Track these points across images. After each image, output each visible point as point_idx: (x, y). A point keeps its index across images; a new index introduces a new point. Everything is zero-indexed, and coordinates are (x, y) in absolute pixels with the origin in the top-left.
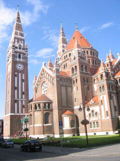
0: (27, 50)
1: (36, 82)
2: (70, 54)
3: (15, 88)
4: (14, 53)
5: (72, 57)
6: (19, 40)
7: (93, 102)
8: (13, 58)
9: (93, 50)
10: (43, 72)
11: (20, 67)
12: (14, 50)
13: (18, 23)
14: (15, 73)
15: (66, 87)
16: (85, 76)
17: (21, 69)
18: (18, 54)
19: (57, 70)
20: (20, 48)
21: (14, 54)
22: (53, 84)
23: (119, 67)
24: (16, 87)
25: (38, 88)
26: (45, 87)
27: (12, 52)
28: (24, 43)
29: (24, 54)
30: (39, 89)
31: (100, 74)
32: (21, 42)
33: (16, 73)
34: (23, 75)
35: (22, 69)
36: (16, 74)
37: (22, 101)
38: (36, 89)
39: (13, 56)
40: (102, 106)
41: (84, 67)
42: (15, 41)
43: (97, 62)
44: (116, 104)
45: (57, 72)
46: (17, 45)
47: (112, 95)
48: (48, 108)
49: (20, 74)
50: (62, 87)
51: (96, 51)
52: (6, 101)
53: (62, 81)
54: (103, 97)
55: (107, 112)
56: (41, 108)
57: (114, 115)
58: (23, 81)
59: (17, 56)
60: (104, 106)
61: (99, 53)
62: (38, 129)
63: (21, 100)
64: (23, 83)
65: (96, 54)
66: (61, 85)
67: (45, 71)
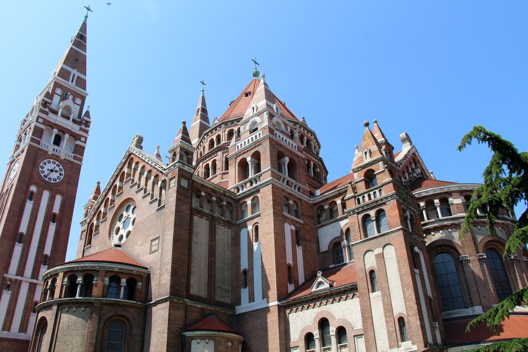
0: (89, 126)
3: (20, 238)
5: (245, 129)
8: (32, 140)
10: (129, 167)
13: (75, 48)
14: (28, 187)
18: (55, 131)
21: (43, 127)
24: (22, 235)
27: (37, 121)
28: (82, 106)
30: (104, 228)
31: (363, 167)
32: (74, 100)
33: (33, 188)
34: (58, 199)
36: (32, 193)
37: (32, 288)
38: (91, 231)
39: (38, 133)
41: (287, 159)
43: (318, 170)
45: (185, 158)
47: (416, 249)
49: (46, 195)
53: (199, 196)
55: (401, 320)
56: (96, 291)
58: (50, 217)
63: (31, 283)
64: (53, 227)
66: (193, 212)
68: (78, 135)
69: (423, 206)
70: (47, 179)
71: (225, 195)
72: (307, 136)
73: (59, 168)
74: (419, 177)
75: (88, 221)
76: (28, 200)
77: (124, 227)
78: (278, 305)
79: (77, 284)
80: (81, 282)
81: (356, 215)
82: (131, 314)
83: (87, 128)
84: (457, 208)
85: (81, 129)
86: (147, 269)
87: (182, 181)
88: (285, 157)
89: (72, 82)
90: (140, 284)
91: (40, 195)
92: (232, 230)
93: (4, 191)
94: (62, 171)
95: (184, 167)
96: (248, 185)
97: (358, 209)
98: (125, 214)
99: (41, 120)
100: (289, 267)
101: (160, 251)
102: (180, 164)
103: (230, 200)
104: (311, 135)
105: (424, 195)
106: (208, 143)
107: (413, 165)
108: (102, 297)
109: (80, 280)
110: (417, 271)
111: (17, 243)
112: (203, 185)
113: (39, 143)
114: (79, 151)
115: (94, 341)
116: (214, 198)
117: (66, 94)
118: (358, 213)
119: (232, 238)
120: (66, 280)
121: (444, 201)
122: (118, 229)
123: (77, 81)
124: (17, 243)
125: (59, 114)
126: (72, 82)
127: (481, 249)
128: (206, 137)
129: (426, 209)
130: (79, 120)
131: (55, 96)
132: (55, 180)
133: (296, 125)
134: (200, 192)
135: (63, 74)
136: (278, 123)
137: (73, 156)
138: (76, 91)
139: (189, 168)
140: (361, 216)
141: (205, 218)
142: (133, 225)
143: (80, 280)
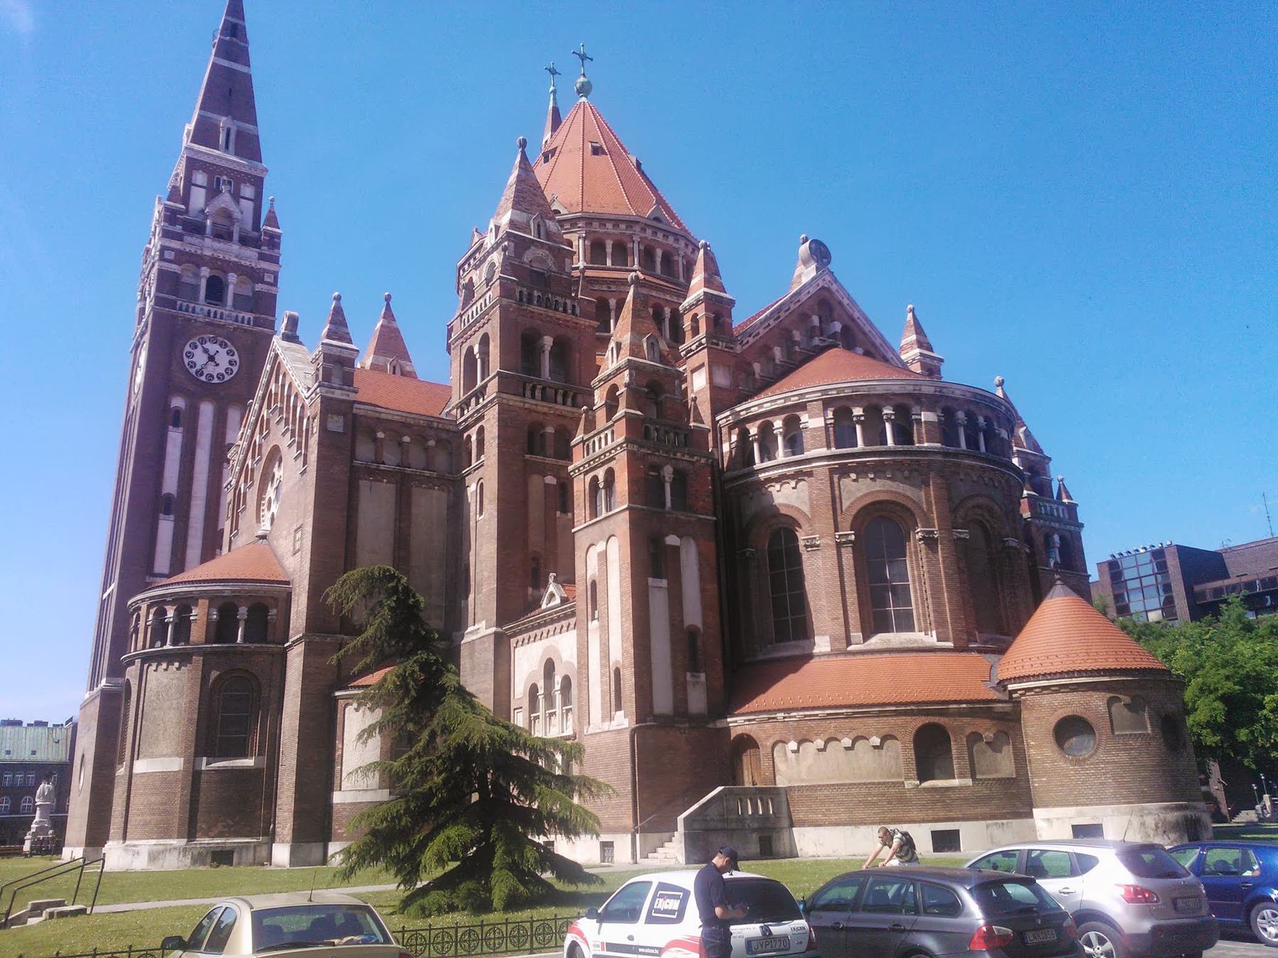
6: (217, 178)
7: (557, 601)
9: (667, 233)
11: (211, 358)
12: (175, 244)
15: (404, 484)
18: (205, 272)
20: (223, 235)
21: (174, 268)
23: (795, 343)
24: (169, 496)
27: (162, 258)
28: (257, 200)
32: (237, 197)
33: (178, 402)
36: (177, 411)
40: (595, 622)
41: (548, 341)
42: (189, 182)
44: (693, 615)
47: (672, 540)
48: (245, 639)
49: (207, 411)
50: (364, 485)
52: (104, 591)
53: (375, 440)
54: (603, 556)
55: (617, 672)
56: (197, 633)
57: (663, 702)
59: (196, 288)
60: (605, 630)
62: (153, 799)
69: (755, 435)
70: (203, 378)
71: (431, 428)
72: (660, 244)
73: (226, 349)
74: (826, 344)
76: (171, 427)
78: (495, 633)
79: (168, 624)
80: (171, 620)
81: (582, 476)
83: (275, 252)
84: (813, 437)
85: (262, 257)
86: (288, 583)
87: (330, 420)
89: (227, 147)
90: (274, 611)
91: (194, 413)
92: (449, 491)
93: (130, 412)
94: (233, 355)
95: (333, 393)
96: (473, 400)
97: (583, 466)
102: (324, 390)
103: (444, 436)
104: (677, 240)
105: (755, 411)
107: (816, 320)
108: (206, 643)
109: (171, 613)
110: (659, 586)
111: (162, 515)
112: (378, 418)
115: (196, 716)
116: (406, 439)
117: (218, 179)
118: (586, 473)
119: (448, 508)
120: (151, 617)
121: (792, 424)
123: (236, 144)
124: (162, 515)
125: (208, 230)
126: (227, 147)
127: (846, 521)
130: (256, 234)
131: (194, 190)
132: (220, 376)
133: (632, 227)
135: (204, 134)
137: (252, 318)
138: (237, 168)
139: (343, 392)
141: (385, 480)
143: (171, 613)
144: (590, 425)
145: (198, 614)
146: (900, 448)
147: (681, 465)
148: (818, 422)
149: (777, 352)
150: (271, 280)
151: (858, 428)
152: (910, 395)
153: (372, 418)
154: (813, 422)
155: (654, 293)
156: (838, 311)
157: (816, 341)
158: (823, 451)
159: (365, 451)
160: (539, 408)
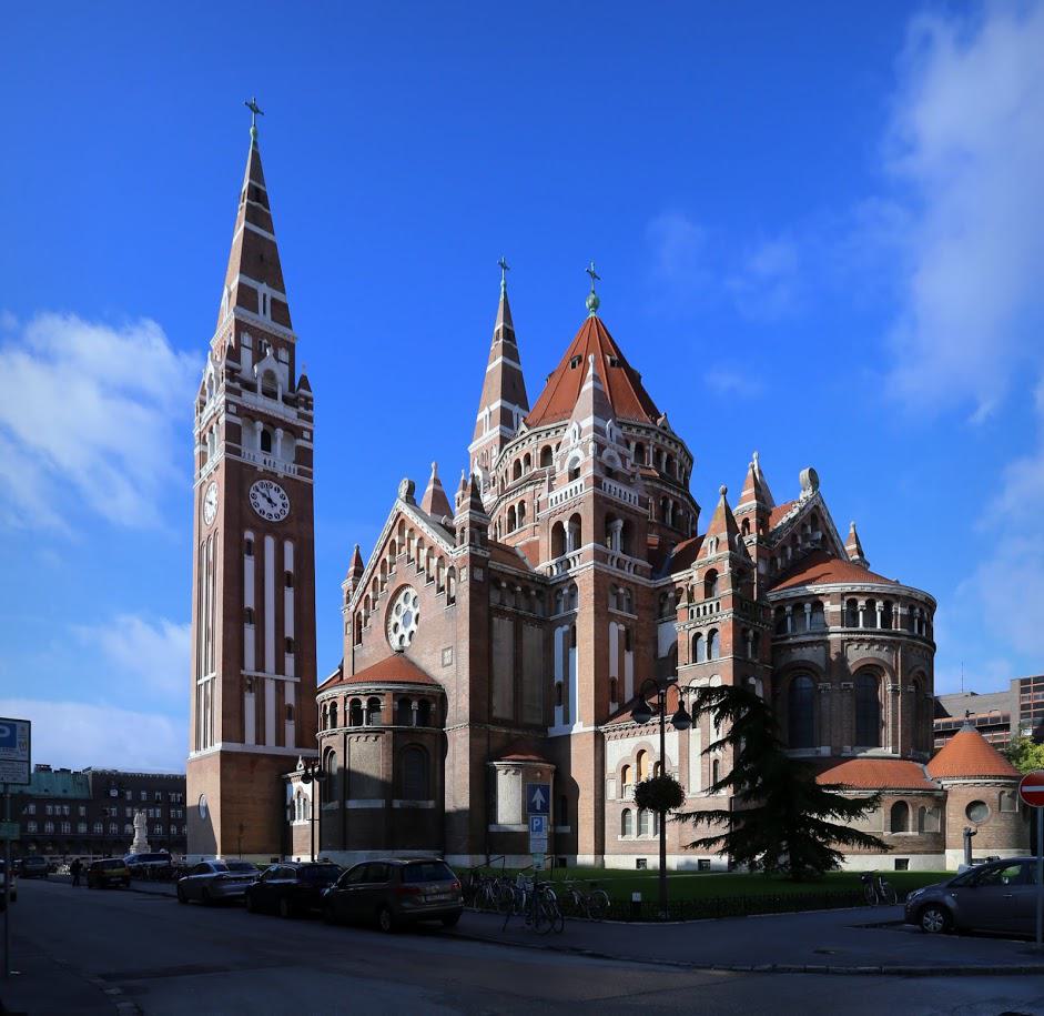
0: (310, 407)
1: (360, 589)
2: (547, 452)
4: (237, 415)
8: (228, 449)
16: (619, 573)
17: (277, 516)
19: (478, 527)
20: (270, 394)
21: (238, 421)
22: (451, 600)
23: (798, 545)
25: (366, 618)
26: (407, 616)
29: (293, 433)
30: (375, 622)
35: (282, 517)
39: (233, 433)
43: (681, 512)
46: (251, 369)
47: (752, 681)
51: (684, 449)
53: (499, 588)
61: (695, 460)
65: (681, 467)
67: (411, 530)
68: (296, 427)
71: (533, 581)
72: (667, 449)
75: (353, 608)
77: (406, 624)
82: (427, 741)
83: (309, 412)
84: (833, 618)
85: (300, 416)
88: (616, 519)
90: (434, 706)
98: (403, 606)
99: (232, 408)
100: (613, 681)
101: (454, 665)
106: (512, 466)
107: (809, 528)
113: (238, 452)
114: (304, 457)
120: (348, 704)
122: (397, 624)
128: (508, 453)
129: (791, 616)
130: (291, 395)
134: (500, 583)
136: (611, 458)
140: (692, 633)
142: (417, 622)
144: (691, 598)
145: (385, 704)
146: (886, 630)
147: (757, 630)
148: (838, 608)
149: (790, 550)
150: (308, 437)
151: (861, 613)
152: (894, 595)
153: (499, 572)
154: (832, 608)
155: (664, 488)
156: (820, 523)
157: (808, 545)
158: (839, 628)
159: (495, 597)
160: (617, 575)
